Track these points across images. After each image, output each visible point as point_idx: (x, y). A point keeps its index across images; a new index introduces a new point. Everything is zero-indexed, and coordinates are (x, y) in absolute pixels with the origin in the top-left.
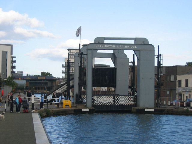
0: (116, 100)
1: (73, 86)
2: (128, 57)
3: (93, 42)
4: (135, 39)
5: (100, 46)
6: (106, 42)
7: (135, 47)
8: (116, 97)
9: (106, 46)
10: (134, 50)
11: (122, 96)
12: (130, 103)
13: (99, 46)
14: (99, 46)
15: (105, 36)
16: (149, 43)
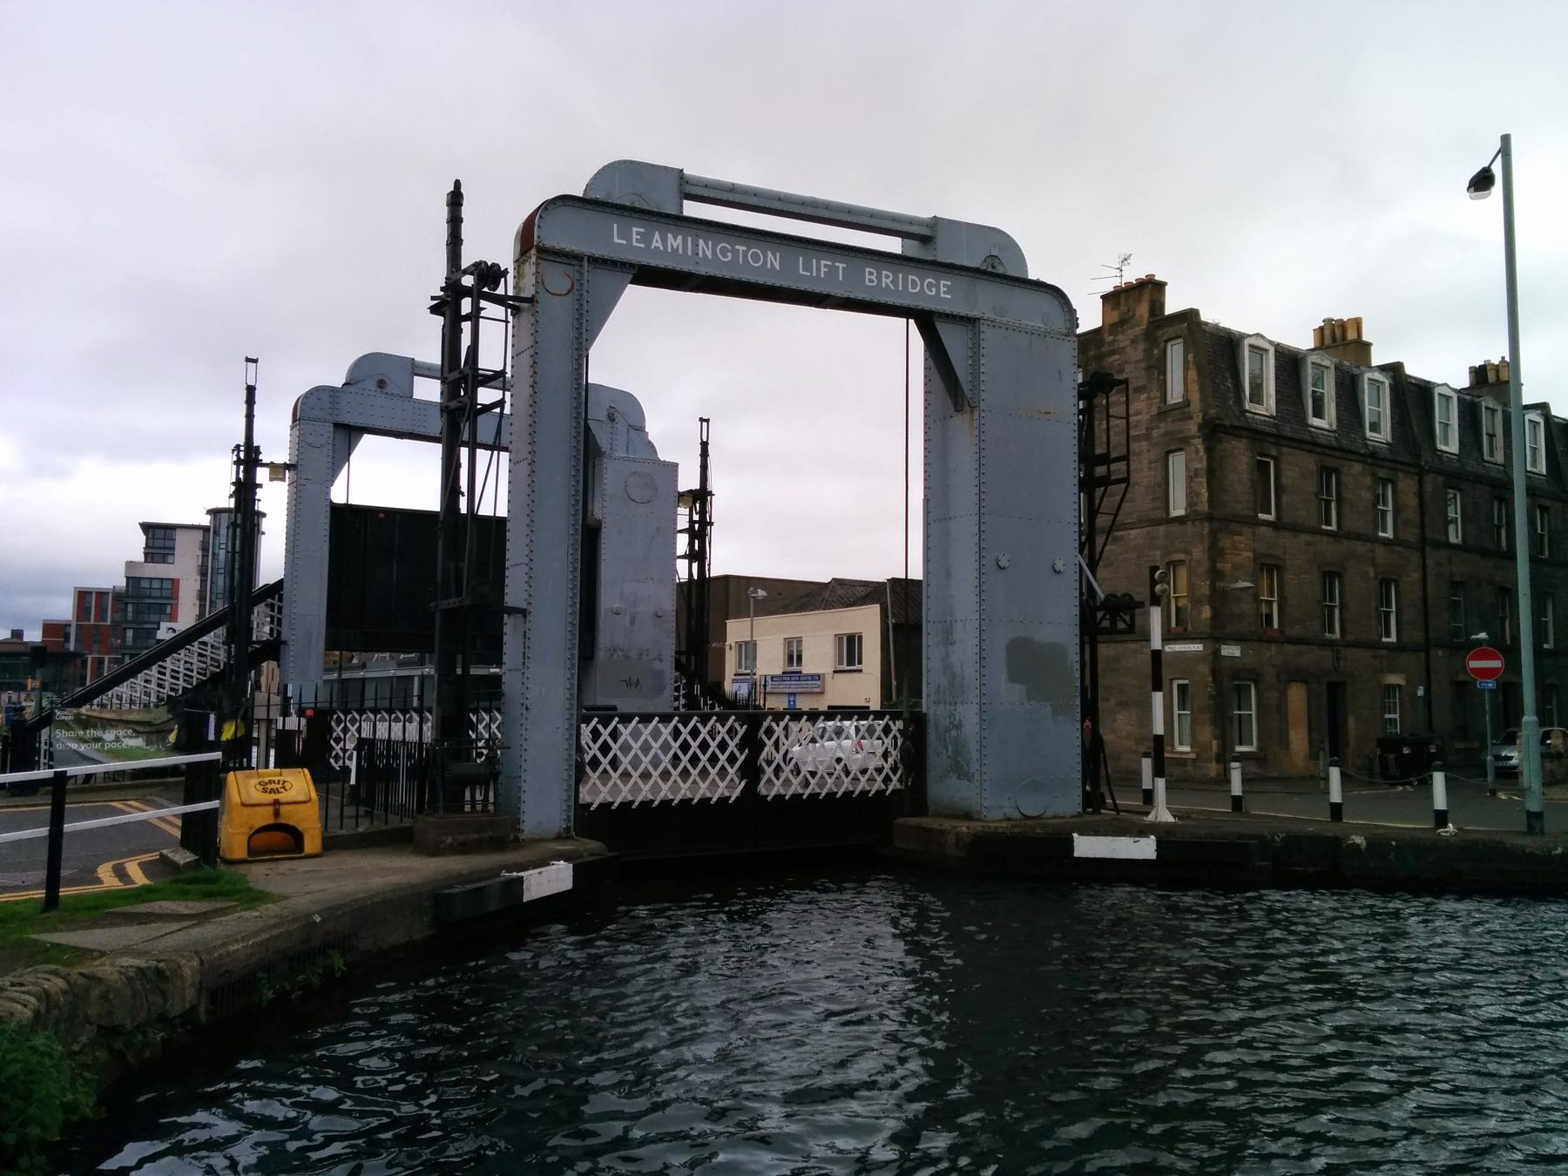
0: (732, 759)
1: (273, 649)
2: (663, 455)
3: (579, 192)
4: (924, 234)
5: (656, 242)
6: (692, 209)
7: (938, 292)
8: (769, 732)
9: (705, 248)
10: (927, 322)
11: (646, 719)
12: (787, 783)
13: (646, 238)
14: (646, 238)
15: (695, 168)
16: (1032, 276)
